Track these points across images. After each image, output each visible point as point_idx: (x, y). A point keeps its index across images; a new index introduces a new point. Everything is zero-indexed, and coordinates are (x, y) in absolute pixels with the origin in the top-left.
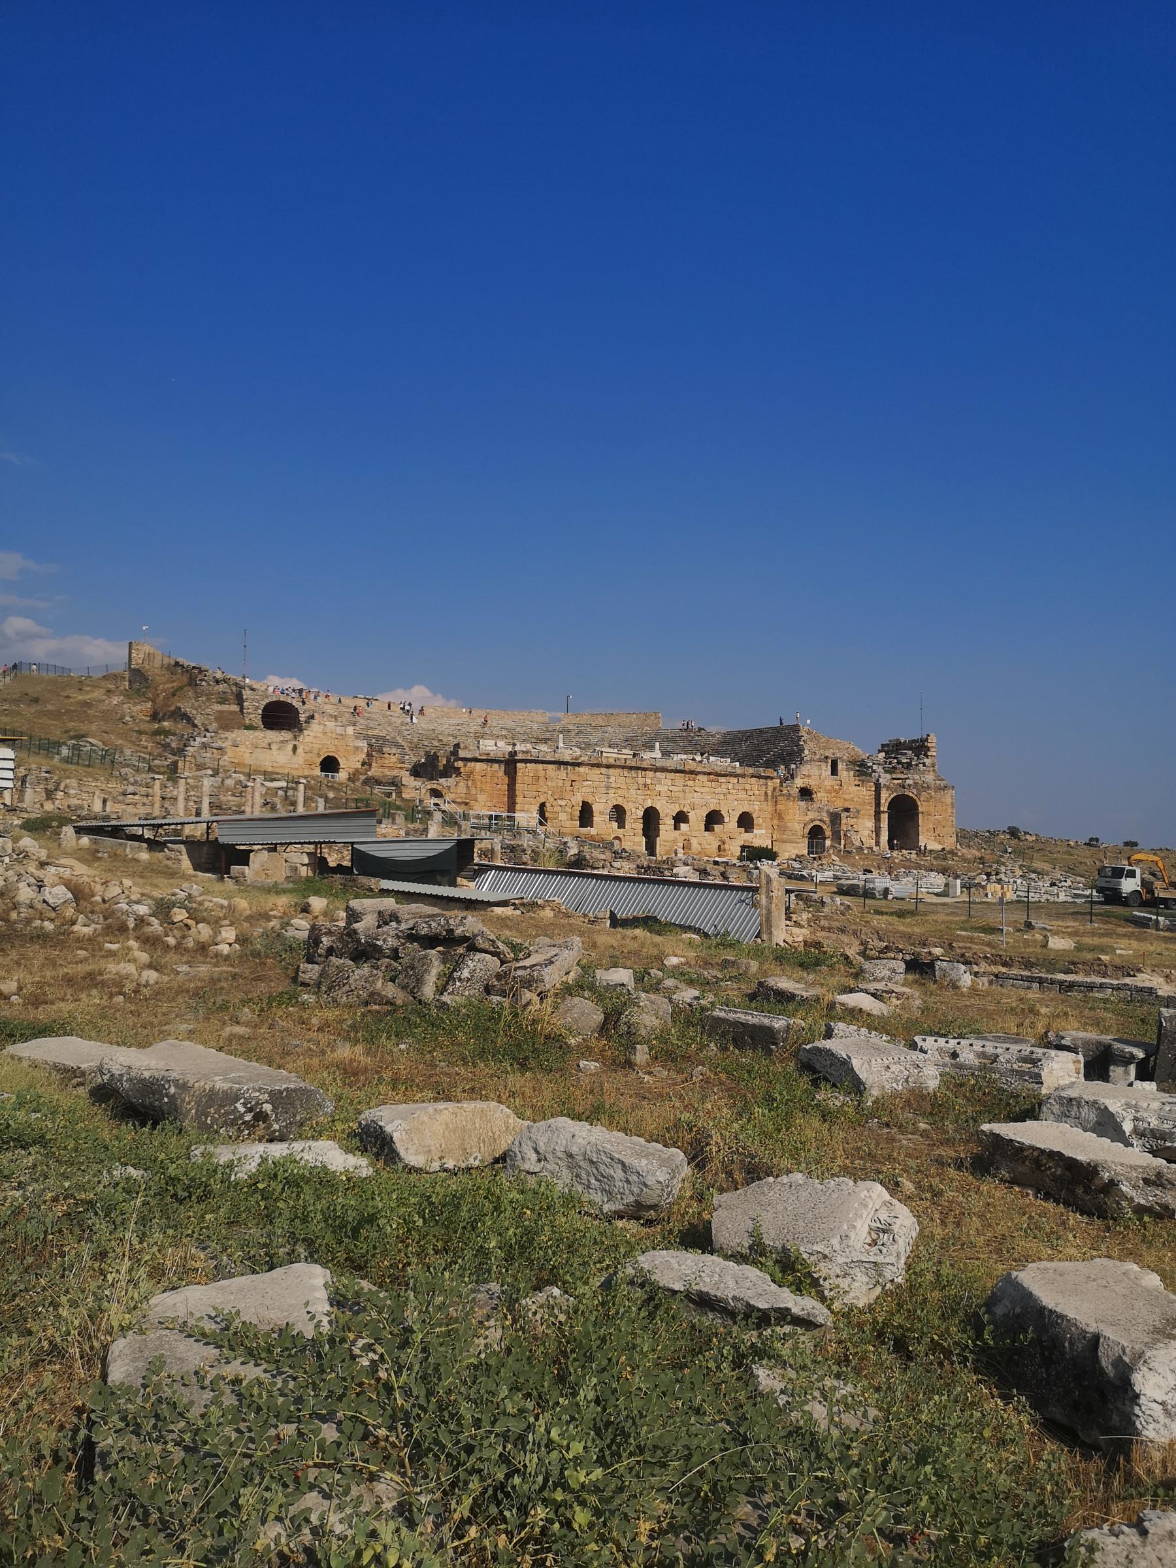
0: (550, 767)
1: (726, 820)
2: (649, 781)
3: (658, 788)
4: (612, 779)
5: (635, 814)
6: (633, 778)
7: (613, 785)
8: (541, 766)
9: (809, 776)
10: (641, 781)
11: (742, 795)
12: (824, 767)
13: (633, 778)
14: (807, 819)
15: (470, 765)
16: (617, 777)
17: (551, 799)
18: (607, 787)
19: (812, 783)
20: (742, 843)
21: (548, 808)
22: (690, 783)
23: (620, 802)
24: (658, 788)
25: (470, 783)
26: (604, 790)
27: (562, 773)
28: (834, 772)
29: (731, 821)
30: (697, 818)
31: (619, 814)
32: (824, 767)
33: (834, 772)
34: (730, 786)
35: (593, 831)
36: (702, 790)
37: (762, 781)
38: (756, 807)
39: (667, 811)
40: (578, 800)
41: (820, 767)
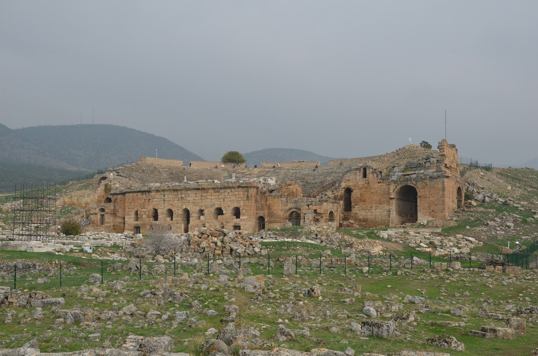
0: (139, 194)
1: (224, 212)
2: (183, 196)
3: (188, 199)
4: (166, 196)
5: (178, 212)
6: (176, 195)
7: (166, 199)
8: (135, 194)
9: (349, 181)
10: (180, 196)
11: (233, 198)
12: (358, 174)
13: (176, 195)
14: (287, 208)
15: (115, 197)
16: (169, 196)
17: (140, 209)
18: (164, 201)
19: (350, 184)
20: (233, 224)
21: (139, 213)
22: (205, 194)
23: (170, 207)
24: (188, 199)
25: (116, 204)
26: (162, 202)
27: (144, 196)
28: (365, 176)
29: (228, 212)
30: (209, 212)
31: (170, 213)
32: (358, 174)
33: (365, 176)
34: (226, 194)
35: (157, 222)
36: (211, 197)
37: (245, 189)
38: (242, 204)
39: (194, 210)
40: (151, 208)
41: (356, 174)
